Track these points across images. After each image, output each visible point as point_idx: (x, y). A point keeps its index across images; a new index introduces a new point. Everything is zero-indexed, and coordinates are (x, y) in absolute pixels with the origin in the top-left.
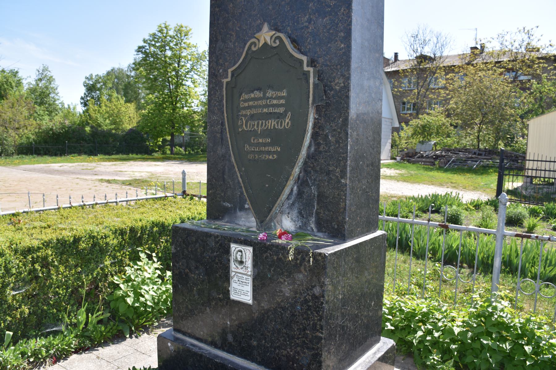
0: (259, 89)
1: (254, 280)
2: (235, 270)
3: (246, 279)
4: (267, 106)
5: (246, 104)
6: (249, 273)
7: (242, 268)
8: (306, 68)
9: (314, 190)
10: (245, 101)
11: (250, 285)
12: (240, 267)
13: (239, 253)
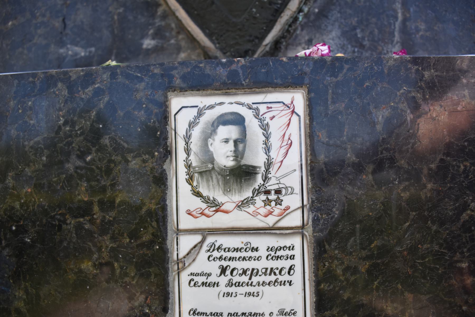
1: (320, 252)
2: (203, 223)
6: (295, 220)
11: (297, 277)
12: (228, 200)
13: (231, 132)
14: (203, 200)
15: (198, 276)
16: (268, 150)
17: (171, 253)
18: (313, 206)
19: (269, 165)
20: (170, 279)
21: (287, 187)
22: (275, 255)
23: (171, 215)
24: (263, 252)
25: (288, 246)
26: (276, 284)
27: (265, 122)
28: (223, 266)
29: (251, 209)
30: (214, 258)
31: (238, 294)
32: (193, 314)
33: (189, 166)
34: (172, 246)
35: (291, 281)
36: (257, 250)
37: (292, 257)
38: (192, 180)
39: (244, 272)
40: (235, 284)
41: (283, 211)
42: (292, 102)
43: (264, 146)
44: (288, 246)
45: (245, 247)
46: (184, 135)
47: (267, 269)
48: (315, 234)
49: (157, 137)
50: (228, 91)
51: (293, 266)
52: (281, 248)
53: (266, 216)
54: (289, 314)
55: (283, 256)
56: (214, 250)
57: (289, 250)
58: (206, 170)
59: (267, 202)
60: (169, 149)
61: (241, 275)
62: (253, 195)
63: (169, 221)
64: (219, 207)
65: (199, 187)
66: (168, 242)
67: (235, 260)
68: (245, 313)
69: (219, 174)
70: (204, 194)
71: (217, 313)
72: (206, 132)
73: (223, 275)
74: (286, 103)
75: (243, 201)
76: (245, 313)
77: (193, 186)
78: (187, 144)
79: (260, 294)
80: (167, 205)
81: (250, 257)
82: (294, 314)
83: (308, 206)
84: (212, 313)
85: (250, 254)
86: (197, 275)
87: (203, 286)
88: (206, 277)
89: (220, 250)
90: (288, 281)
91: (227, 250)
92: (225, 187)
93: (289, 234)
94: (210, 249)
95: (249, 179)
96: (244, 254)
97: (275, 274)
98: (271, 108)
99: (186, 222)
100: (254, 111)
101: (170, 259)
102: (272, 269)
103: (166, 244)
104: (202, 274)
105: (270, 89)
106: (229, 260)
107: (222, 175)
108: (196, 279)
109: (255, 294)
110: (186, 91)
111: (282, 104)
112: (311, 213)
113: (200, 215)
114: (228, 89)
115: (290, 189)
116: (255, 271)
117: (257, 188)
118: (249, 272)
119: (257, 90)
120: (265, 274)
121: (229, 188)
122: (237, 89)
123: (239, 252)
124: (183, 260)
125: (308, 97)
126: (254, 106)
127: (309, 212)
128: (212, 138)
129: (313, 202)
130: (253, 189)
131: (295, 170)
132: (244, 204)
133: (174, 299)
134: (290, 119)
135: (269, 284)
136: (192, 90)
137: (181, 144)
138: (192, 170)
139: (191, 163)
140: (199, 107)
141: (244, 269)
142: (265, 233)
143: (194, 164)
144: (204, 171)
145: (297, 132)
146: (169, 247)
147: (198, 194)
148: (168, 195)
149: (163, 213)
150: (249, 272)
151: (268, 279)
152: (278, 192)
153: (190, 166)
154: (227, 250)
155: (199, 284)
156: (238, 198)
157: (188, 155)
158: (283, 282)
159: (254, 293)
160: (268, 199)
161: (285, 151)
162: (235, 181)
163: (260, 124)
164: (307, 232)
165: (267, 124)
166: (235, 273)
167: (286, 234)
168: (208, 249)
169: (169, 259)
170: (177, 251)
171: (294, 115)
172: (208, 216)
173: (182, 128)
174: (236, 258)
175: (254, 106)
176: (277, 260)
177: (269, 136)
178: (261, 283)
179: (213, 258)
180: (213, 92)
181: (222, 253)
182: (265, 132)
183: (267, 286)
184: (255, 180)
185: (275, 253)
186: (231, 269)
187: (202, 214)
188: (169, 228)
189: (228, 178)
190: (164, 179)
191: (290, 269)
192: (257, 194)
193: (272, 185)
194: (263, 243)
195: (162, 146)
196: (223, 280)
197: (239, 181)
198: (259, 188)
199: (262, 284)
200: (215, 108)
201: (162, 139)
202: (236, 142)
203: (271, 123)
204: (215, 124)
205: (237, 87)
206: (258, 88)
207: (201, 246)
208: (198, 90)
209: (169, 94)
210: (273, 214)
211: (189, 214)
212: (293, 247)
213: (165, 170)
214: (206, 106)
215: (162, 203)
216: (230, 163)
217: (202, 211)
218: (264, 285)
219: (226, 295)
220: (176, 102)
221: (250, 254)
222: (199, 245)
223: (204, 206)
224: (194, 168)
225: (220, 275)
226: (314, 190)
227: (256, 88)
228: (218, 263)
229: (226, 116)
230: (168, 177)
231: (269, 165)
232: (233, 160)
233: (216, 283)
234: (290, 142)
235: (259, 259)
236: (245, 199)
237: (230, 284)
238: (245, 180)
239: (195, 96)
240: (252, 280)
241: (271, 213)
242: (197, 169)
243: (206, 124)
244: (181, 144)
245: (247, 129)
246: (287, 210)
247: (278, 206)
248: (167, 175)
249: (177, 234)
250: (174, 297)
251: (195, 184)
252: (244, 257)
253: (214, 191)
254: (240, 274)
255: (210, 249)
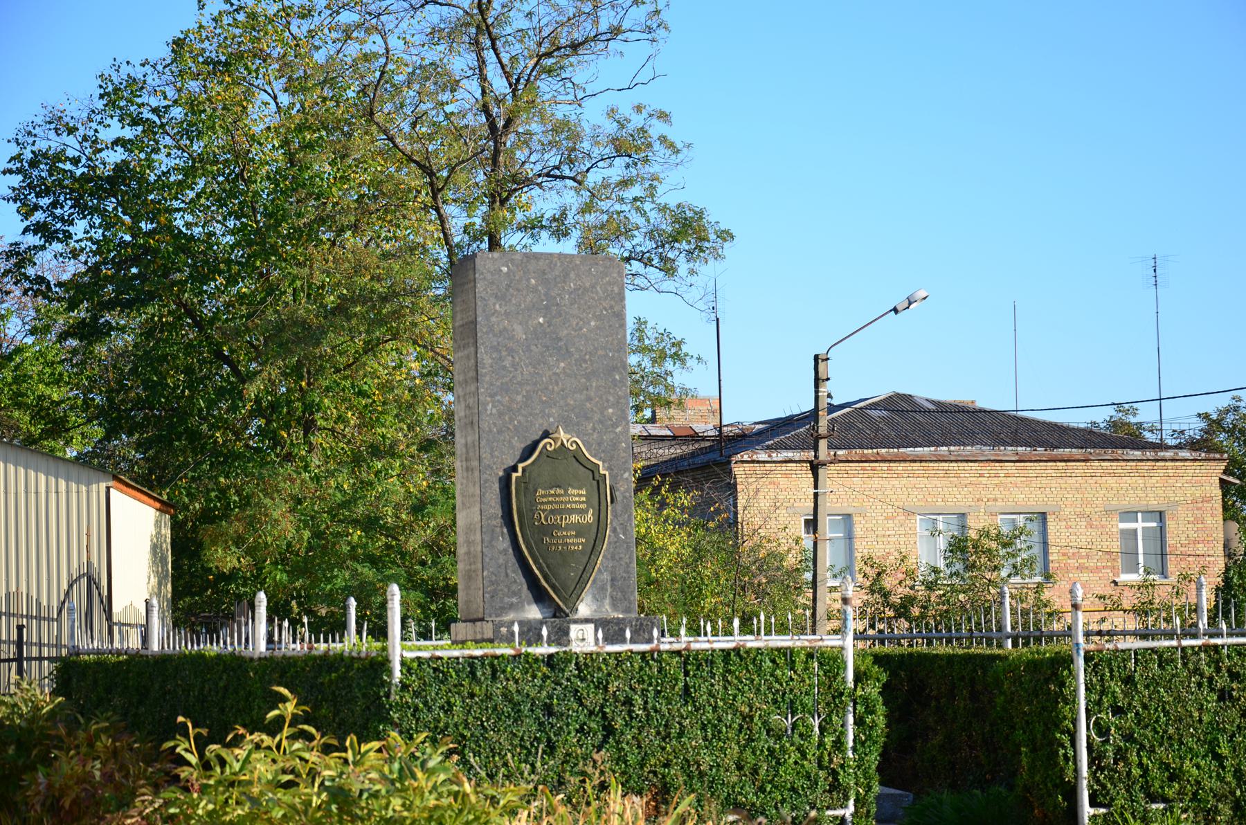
0: (559, 487)
4: (569, 502)
5: (544, 500)
8: (602, 472)
9: (606, 576)
10: (543, 496)
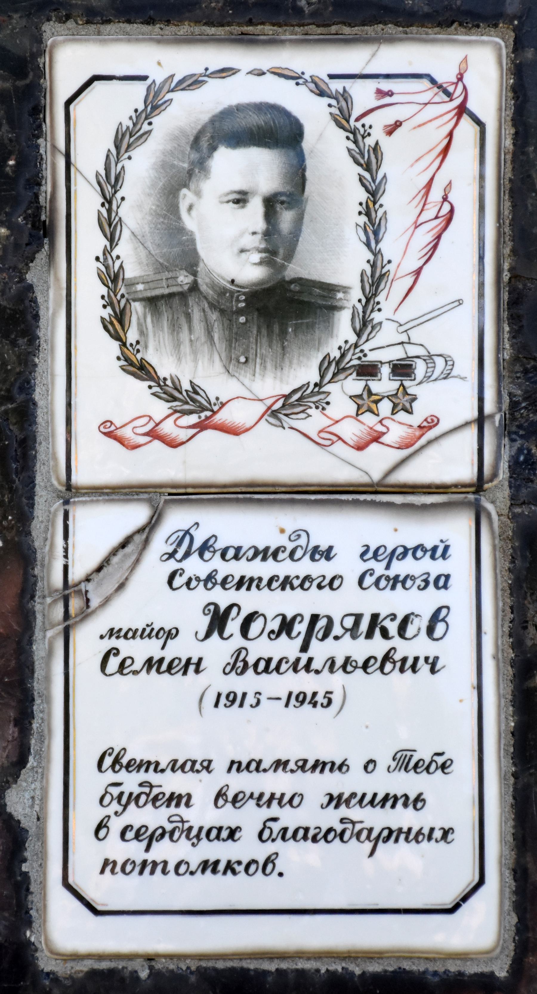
3: (383, 566)
6: (453, 461)
7: (286, 408)
11: (456, 647)
12: (245, 392)
13: (255, 168)
14: (157, 389)
15: (133, 637)
16: (376, 233)
17: (43, 566)
18: (513, 419)
19: (375, 281)
20: (39, 650)
21: (430, 356)
22: (387, 573)
23: (46, 439)
24: (347, 564)
25: (429, 546)
26: (388, 667)
27: (370, 141)
28: (216, 606)
29: (315, 421)
30: (190, 579)
31: (263, 698)
32: (113, 766)
33: (112, 278)
34: (49, 540)
35: (436, 658)
36: (328, 554)
37: (442, 582)
38: (121, 322)
39: (286, 626)
40: (256, 665)
41: (418, 433)
42: (460, 78)
43: (363, 219)
44: (429, 546)
45: (290, 546)
46: (97, 174)
47: (358, 618)
48: (518, 510)
49: (7, 176)
50: (250, 29)
51: (444, 612)
52: (406, 550)
53: (360, 447)
54: (427, 769)
55: (413, 578)
56: (187, 554)
57: (433, 557)
58: (177, 293)
59: (365, 403)
60: (43, 217)
61: (274, 635)
62: (322, 377)
63: (41, 456)
64: (208, 413)
65: (146, 347)
66: (37, 527)
67: (258, 587)
68: (287, 762)
69: (213, 306)
70: (162, 373)
71: (194, 762)
72: (173, 166)
73: (216, 635)
74: (440, 80)
75: (287, 397)
76: (287, 762)
77: (124, 344)
78: (110, 202)
79: (337, 698)
80: (35, 404)
81: (307, 578)
82: (443, 767)
83: (497, 418)
84: (175, 761)
85: (305, 567)
86: (130, 634)
87: (148, 671)
88: (162, 641)
89: (207, 555)
90: (427, 659)
91: (231, 553)
92: (230, 348)
93: (433, 506)
94: (175, 551)
95: (311, 327)
96: (285, 568)
97: (385, 634)
98: (390, 94)
99: (96, 463)
100: (333, 102)
101: (39, 584)
102: (375, 617)
103: (29, 533)
104: (148, 633)
105: (391, 29)
106: (239, 585)
107: (222, 312)
108: (127, 648)
109: (320, 698)
110: (109, 22)
111: (426, 84)
112: (506, 441)
113: (148, 439)
114: (250, 23)
115: (440, 362)
116: (322, 623)
117: (336, 354)
118: (301, 628)
119: (347, 30)
120: (353, 632)
121: (245, 352)
122: (280, 25)
123: (270, 560)
124: (83, 586)
125: (513, 62)
126: (336, 86)
127: (499, 437)
128: (192, 186)
129: (514, 405)
130: (321, 358)
131: (460, 302)
132: (293, 406)
133: (48, 721)
134: (451, 135)
135: (365, 666)
136: (129, 22)
137: (87, 204)
138: (123, 291)
139: (121, 267)
140: (149, 81)
141: (284, 617)
142: (356, 503)
143: (130, 273)
144: (163, 296)
145: (470, 178)
146: (37, 544)
147: (141, 370)
148: (39, 369)
149: (22, 429)
150: (301, 628)
151: (361, 649)
152: (402, 369)
153: (116, 276)
154: (231, 553)
155: (137, 666)
156: (271, 385)
157: (112, 240)
158: (410, 662)
159: (315, 694)
160: (370, 393)
161: (429, 237)
162: (264, 331)
163: (352, 146)
164: (493, 502)
165: (376, 148)
166: (255, 628)
167: (424, 507)
168: (170, 549)
169: (35, 584)
170: (66, 557)
171: (466, 121)
172: (173, 444)
173: (91, 151)
174: (260, 579)
175: (336, 86)
176: (393, 588)
177: (378, 188)
178: (339, 662)
179: (184, 579)
180: (197, 29)
181: (217, 563)
182: (367, 175)
183: (359, 672)
184: (329, 327)
185: (388, 567)
186: (244, 614)
187: (154, 434)
188: (39, 479)
189: (242, 319)
190: (29, 317)
191: (435, 618)
192: (335, 375)
193: (383, 347)
194: (348, 532)
195: (24, 206)
196: (217, 651)
197: (276, 328)
198: (343, 356)
199: (344, 667)
200: (205, 88)
201: (22, 182)
202: (271, 204)
203: (386, 143)
204: (204, 143)
205: (281, 20)
206: (350, 25)
207: (146, 542)
208: (150, 21)
209: (47, 27)
210: (383, 439)
211: (109, 435)
212: (446, 548)
213: (30, 288)
214: (176, 80)
215: (20, 398)
216: (250, 272)
217: (151, 425)
218: (349, 668)
219: (223, 700)
220: (71, 59)
221: (305, 567)
222: (139, 539)
223: (160, 409)
224: (131, 284)
225: (208, 635)
226: (518, 368)
227: (344, 24)
228: (202, 596)
229: (241, 115)
230: (41, 313)
231: (375, 281)
232: (261, 263)
233: (195, 660)
234: (446, 208)
235: (336, 583)
236: (295, 391)
237: (239, 665)
238: (296, 329)
239: (138, 40)
240: (311, 652)
241: (376, 438)
242: (140, 287)
243: (175, 138)
244: (87, 204)
245: (309, 163)
246: (430, 428)
247: (402, 416)
248: (37, 306)
249: (67, 502)
250: (49, 714)
251: (132, 336)
252: (287, 578)
253: (195, 360)
254: (272, 632)
255: (175, 551)
